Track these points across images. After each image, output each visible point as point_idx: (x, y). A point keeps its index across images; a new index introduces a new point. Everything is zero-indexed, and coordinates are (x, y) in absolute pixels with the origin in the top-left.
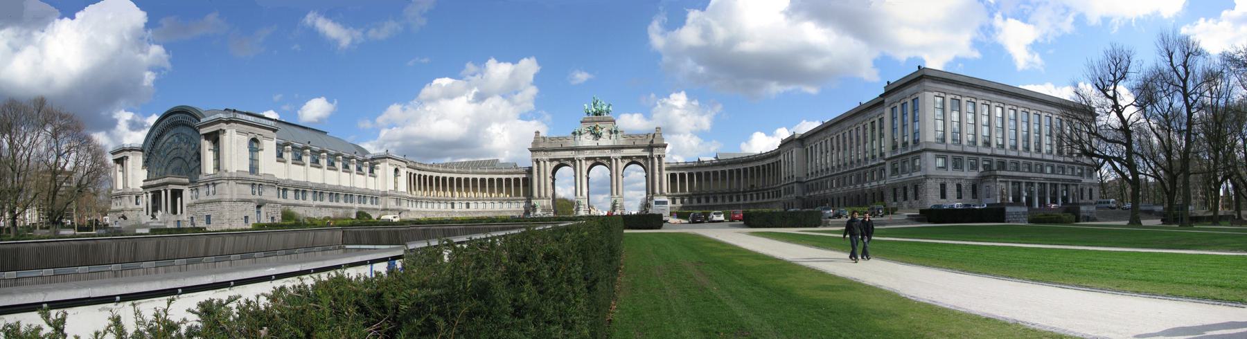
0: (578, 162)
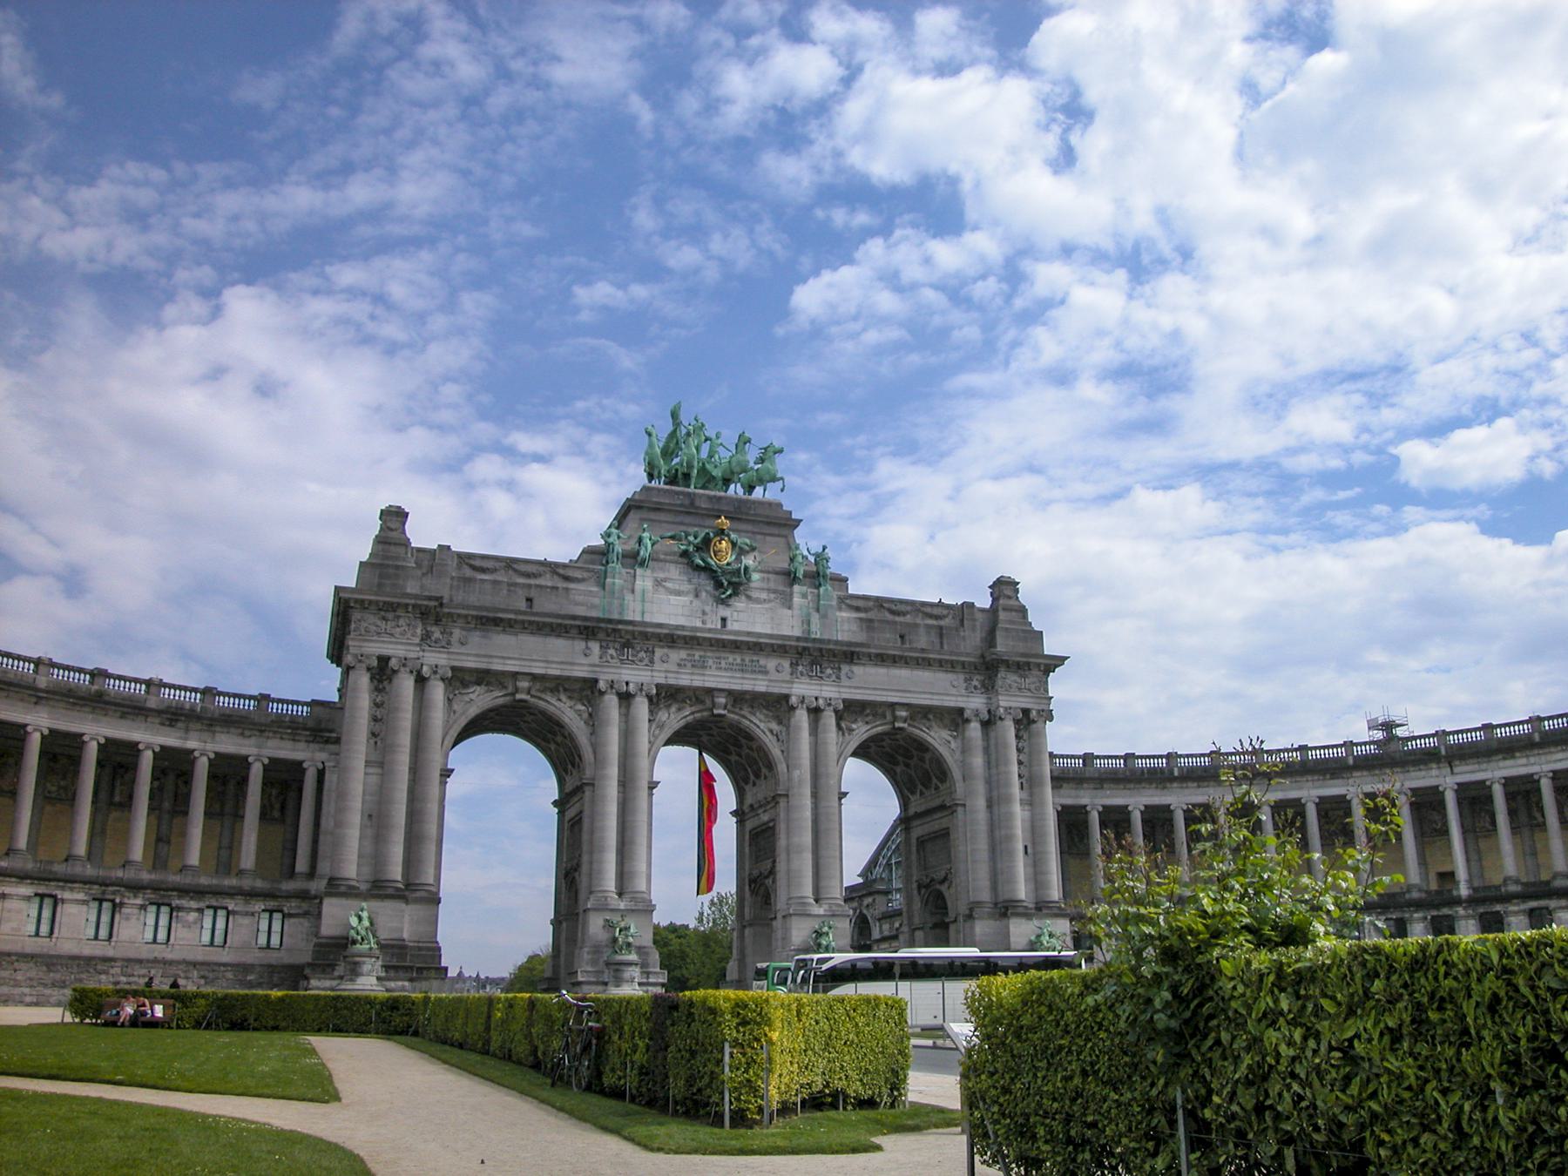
0: (611, 701)
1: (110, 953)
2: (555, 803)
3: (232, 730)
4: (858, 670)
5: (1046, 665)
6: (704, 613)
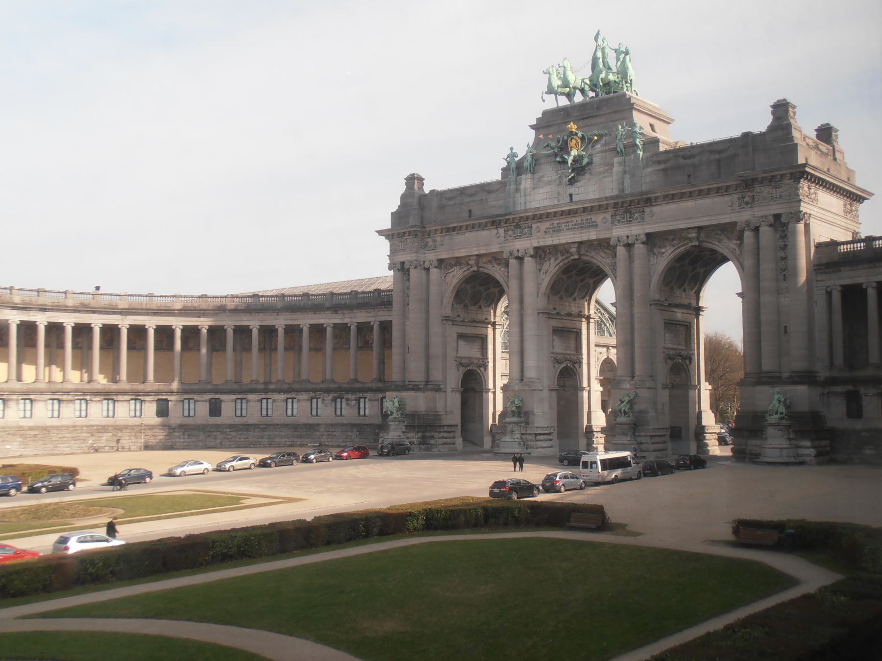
3: (362, 311)
4: (656, 209)
6: (559, 194)
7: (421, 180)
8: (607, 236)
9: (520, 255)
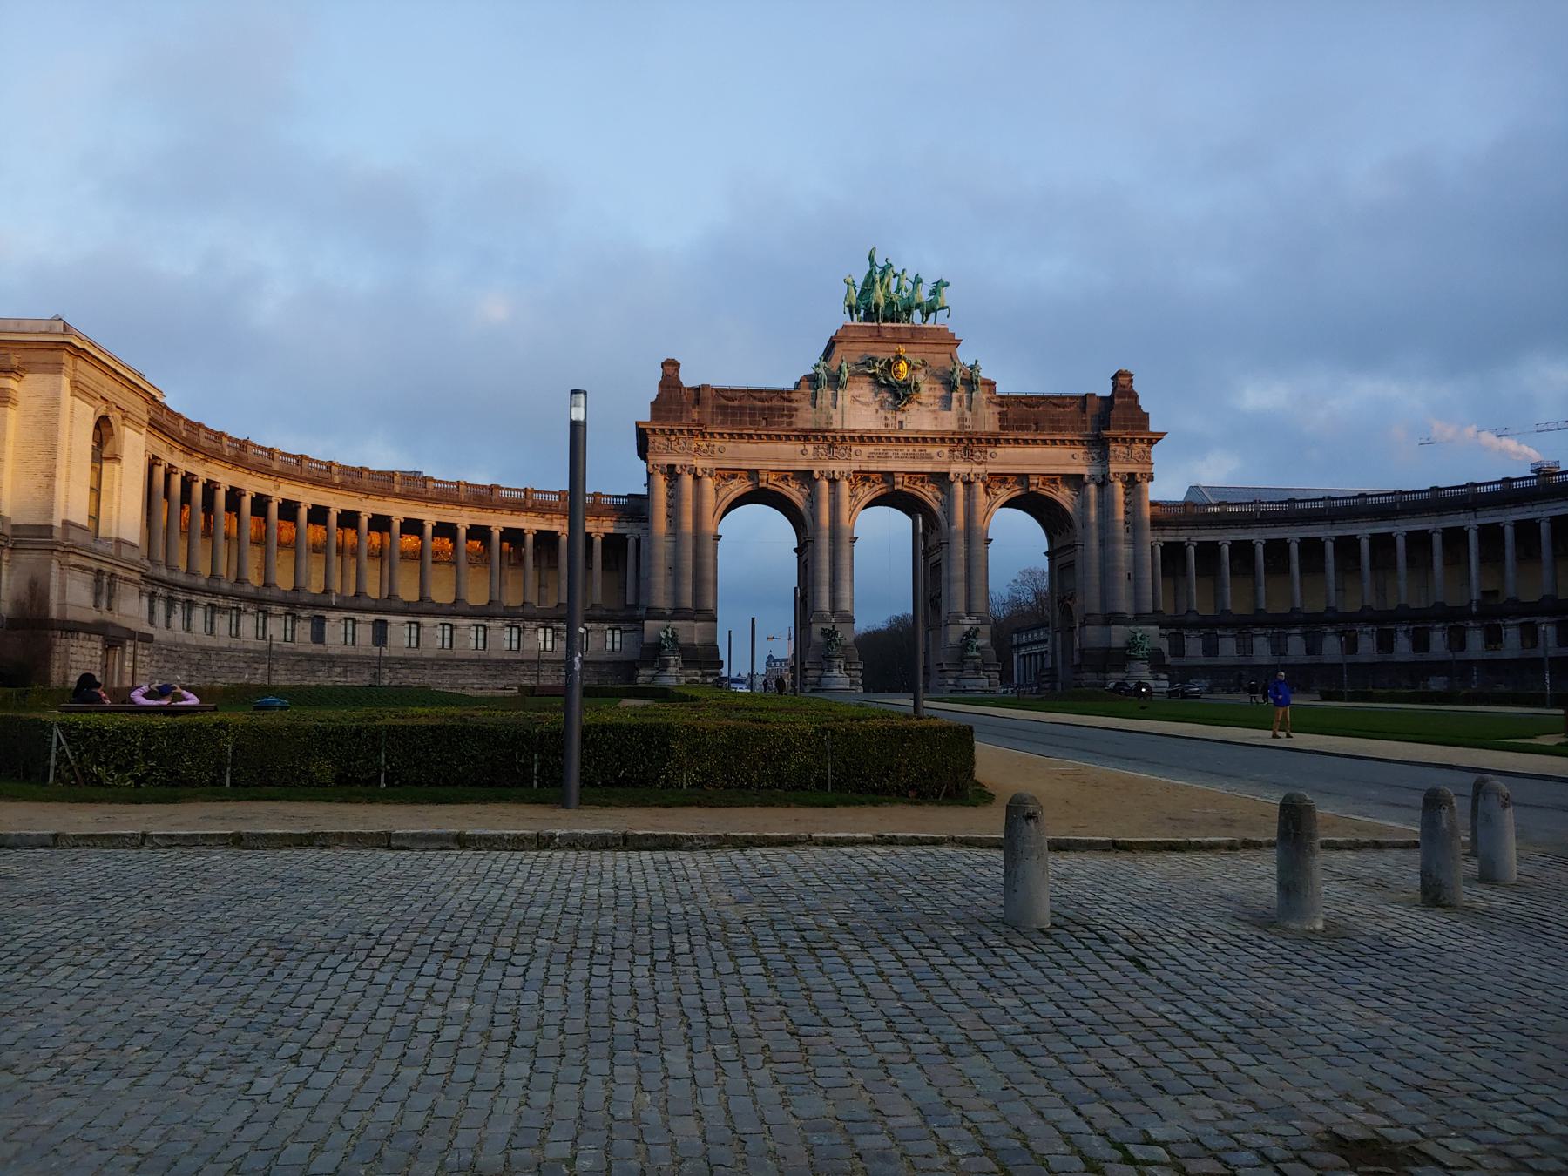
0: (825, 484)
1: (520, 658)
2: (795, 550)
5: (1148, 439)
6: (886, 418)
7: (678, 365)
8: (945, 470)
9: (837, 476)
